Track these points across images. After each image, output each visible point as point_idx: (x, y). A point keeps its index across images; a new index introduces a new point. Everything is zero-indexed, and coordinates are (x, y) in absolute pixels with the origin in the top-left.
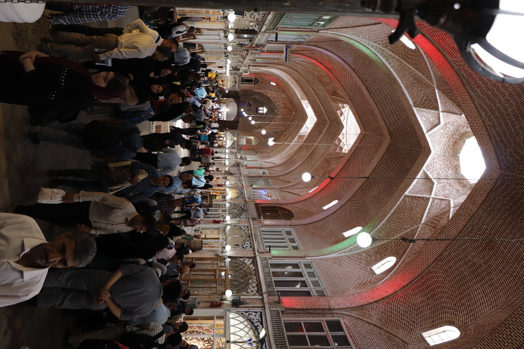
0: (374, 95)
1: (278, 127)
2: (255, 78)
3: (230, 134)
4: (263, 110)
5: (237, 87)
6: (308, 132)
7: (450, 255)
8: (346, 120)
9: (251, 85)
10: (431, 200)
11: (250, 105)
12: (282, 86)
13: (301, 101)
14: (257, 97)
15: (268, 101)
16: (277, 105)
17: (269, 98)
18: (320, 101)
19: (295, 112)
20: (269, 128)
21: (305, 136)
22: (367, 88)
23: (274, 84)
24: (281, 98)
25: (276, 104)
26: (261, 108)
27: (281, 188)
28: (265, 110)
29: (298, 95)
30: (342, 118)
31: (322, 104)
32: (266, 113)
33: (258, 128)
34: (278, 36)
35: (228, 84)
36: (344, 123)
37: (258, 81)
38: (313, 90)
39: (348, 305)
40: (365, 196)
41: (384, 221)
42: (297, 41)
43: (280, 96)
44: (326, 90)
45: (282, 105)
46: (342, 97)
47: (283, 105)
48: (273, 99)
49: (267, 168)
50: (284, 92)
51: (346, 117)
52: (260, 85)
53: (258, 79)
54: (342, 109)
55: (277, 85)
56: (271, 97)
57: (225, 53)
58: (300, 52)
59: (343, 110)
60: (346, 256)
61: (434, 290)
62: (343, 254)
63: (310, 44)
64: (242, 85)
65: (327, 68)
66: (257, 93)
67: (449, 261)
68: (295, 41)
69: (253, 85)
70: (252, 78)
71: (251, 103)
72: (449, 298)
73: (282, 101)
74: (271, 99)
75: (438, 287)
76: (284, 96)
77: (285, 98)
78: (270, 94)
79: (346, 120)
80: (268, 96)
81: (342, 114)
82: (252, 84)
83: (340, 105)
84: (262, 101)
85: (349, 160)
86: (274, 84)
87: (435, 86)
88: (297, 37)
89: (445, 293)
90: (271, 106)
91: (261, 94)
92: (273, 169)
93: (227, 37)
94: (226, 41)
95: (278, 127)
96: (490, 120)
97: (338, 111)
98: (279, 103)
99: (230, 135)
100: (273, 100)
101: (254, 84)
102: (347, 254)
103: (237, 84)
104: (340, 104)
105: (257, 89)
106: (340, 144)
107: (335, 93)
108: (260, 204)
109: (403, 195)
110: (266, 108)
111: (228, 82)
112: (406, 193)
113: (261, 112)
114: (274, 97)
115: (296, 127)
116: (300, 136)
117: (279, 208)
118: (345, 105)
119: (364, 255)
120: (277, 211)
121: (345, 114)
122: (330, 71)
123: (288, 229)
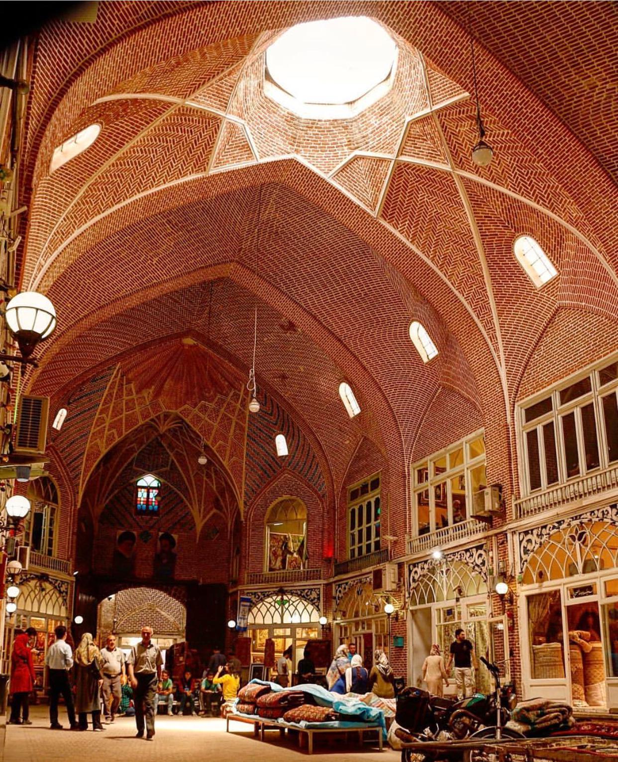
1: (234, 419)
3: (255, 610)
4: (148, 489)
5: (63, 576)
11: (128, 536)
13: (212, 171)
14: (98, 510)
16: (145, 418)
19: (188, 333)
20: (232, 456)
24: (119, 396)
25: (141, 422)
26: (142, 495)
28: (149, 480)
29: (182, 180)
32: (159, 475)
33: (218, 506)
35: (50, 612)
43: (110, 395)
45: (150, 392)
47: (145, 393)
48: (120, 434)
50: (98, 372)
52: (59, 479)
55: (65, 404)
56: (110, 439)
64: (55, 552)
71: (121, 532)
73: (130, 393)
74: (117, 440)
77: (122, 376)
80: (104, 451)
84: (112, 491)
90: (136, 454)
95: (234, 419)
98: (137, 409)
99: (264, 610)
100: (125, 433)
103: (51, 572)
110: (141, 474)
114: (111, 427)
115: (284, 289)
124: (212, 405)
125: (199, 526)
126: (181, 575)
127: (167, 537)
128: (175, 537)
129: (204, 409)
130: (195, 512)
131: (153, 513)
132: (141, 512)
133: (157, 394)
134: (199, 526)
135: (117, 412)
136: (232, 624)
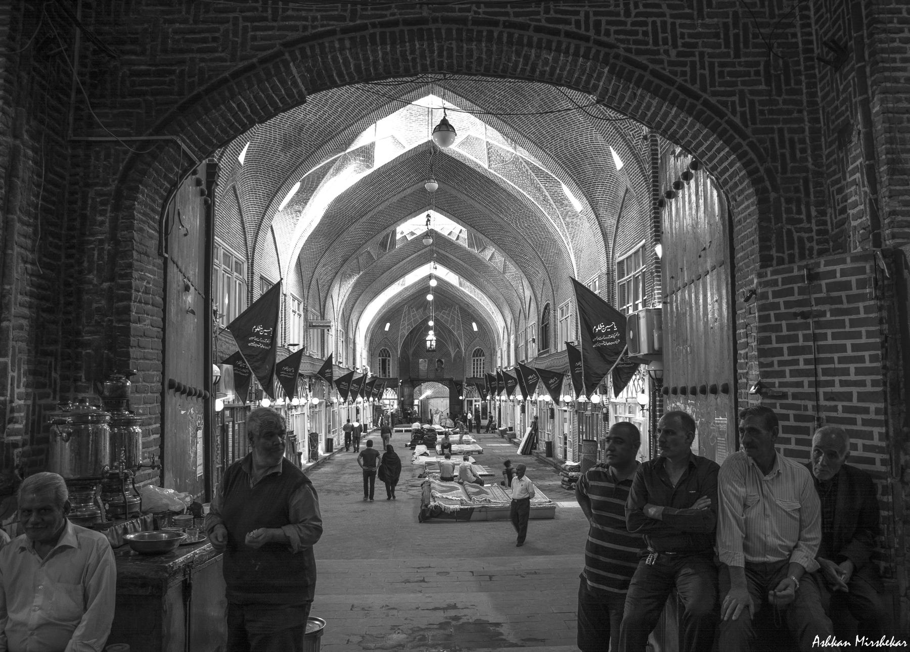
0: (370, 206)
2: (379, 356)
4: (431, 341)
7: (534, 133)
9: (391, 361)
10: (488, 140)
12: (391, 314)
14: (411, 352)
15: (417, 334)
17: (411, 332)
18: (400, 261)
22: (362, 217)
23: (388, 325)
24: (409, 314)
26: (428, 344)
27: (525, 317)
31: (403, 260)
34: (291, 343)
37: (384, 350)
38: (383, 273)
39: (604, 251)
40: (508, 208)
41: (525, 193)
42: (302, 313)
44: (378, 259)
46: (388, 235)
49: (509, 335)
51: (416, 227)
52: (390, 348)
56: (408, 329)
57: (326, 406)
58: (322, 304)
60: (572, 242)
61: (575, 151)
62: (570, 245)
63: (306, 296)
65: (342, 265)
66: (403, 351)
67: (541, 133)
68: (302, 316)
69: (391, 359)
72: (581, 135)
75: (572, 146)
76: (406, 308)
78: (404, 331)
81: (412, 233)
83: (398, 236)
85: (470, 225)
86: (388, 325)
87: (343, 153)
88: (296, 315)
89: (576, 139)
91: (406, 345)
92: (509, 327)
93: (295, 406)
94: (305, 407)
96: (371, 104)
101: (389, 356)
102: (570, 240)
105: (397, 352)
107: (383, 245)
108: (539, 351)
109: (489, 170)
111: (388, 397)
112: (486, 167)
113: (434, 343)
114: (408, 325)
116: (460, 284)
117: (543, 323)
119: (567, 219)
120: (546, 326)
122: (347, 259)
123: (559, 312)
124: (447, 312)
125: (453, 355)
126: (446, 376)
127: (440, 361)
128: (443, 360)
129: (444, 313)
130: (450, 349)
131: (434, 351)
132: (428, 351)
133: (424, 310)
134: (453, 355)
135: (409, 319)
136: (461, 398)
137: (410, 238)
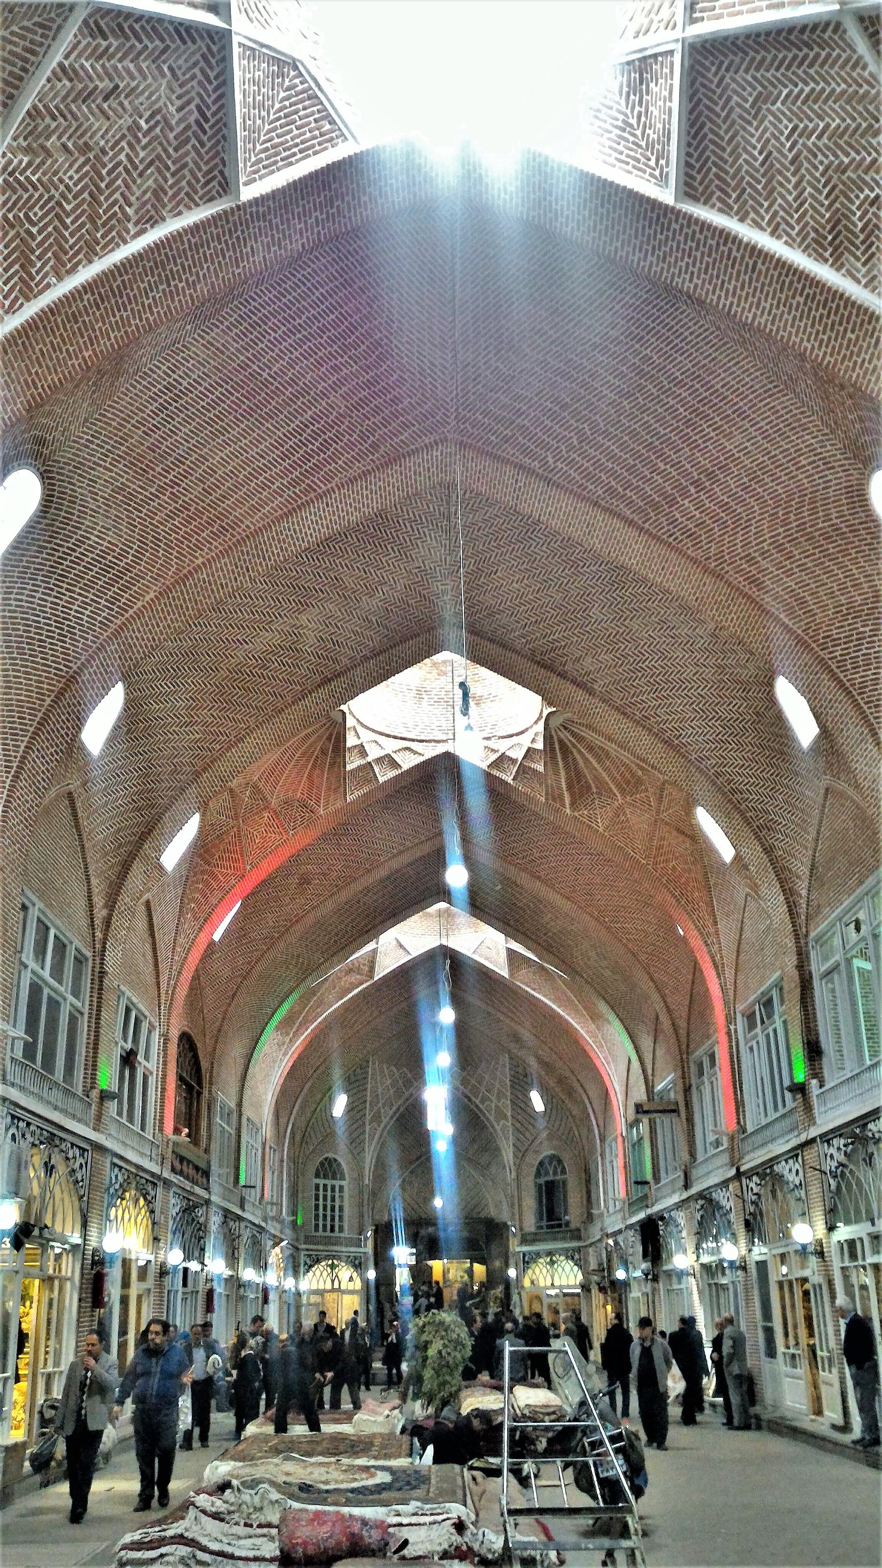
2: (317, 1176)
6: (499, 937)
8: (414, 746)
21: (509, 950)
30: (408, 762)
36: (430, 752)
53: (322, 1164)
54: (369, 759)
59: (374, 753)
70: (317, 1187)
79: (414, 746)
81: (389, 761)
82: (341, 1188)
97: (381, 779)
104: (349, 767)
106: (513, 761)
118: (351, 741)
121: (390, 746)
137: (384, 776)
